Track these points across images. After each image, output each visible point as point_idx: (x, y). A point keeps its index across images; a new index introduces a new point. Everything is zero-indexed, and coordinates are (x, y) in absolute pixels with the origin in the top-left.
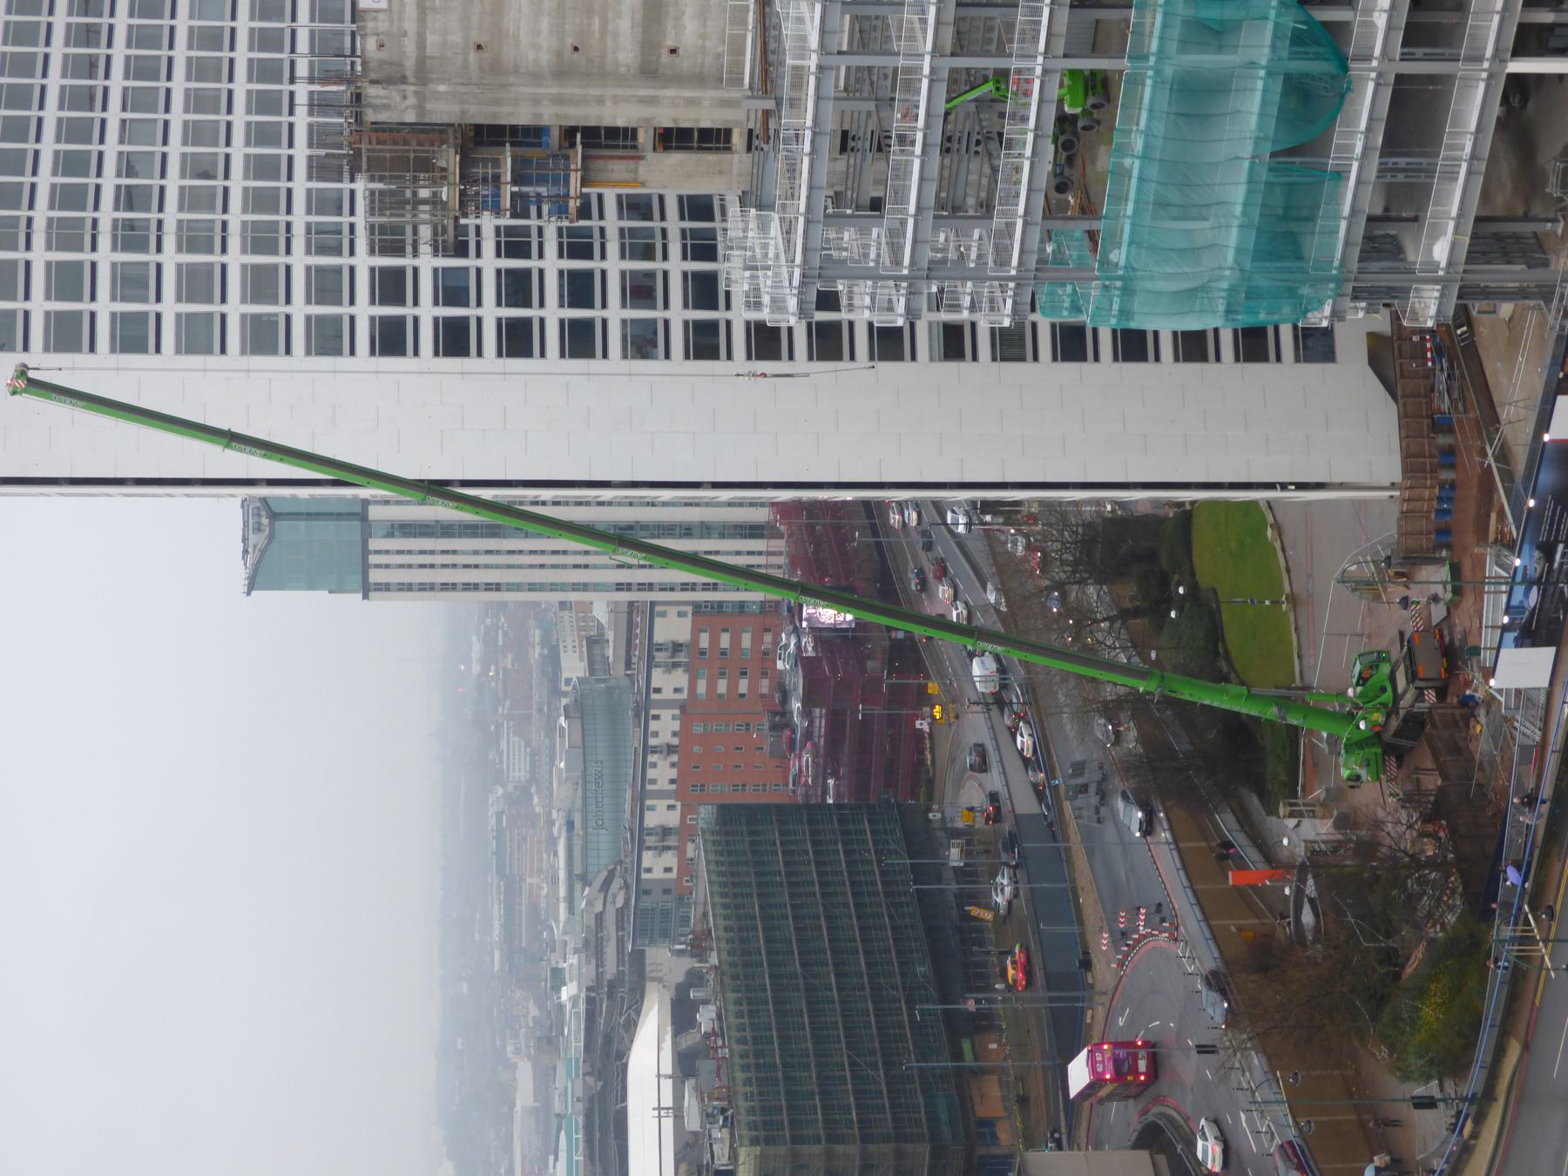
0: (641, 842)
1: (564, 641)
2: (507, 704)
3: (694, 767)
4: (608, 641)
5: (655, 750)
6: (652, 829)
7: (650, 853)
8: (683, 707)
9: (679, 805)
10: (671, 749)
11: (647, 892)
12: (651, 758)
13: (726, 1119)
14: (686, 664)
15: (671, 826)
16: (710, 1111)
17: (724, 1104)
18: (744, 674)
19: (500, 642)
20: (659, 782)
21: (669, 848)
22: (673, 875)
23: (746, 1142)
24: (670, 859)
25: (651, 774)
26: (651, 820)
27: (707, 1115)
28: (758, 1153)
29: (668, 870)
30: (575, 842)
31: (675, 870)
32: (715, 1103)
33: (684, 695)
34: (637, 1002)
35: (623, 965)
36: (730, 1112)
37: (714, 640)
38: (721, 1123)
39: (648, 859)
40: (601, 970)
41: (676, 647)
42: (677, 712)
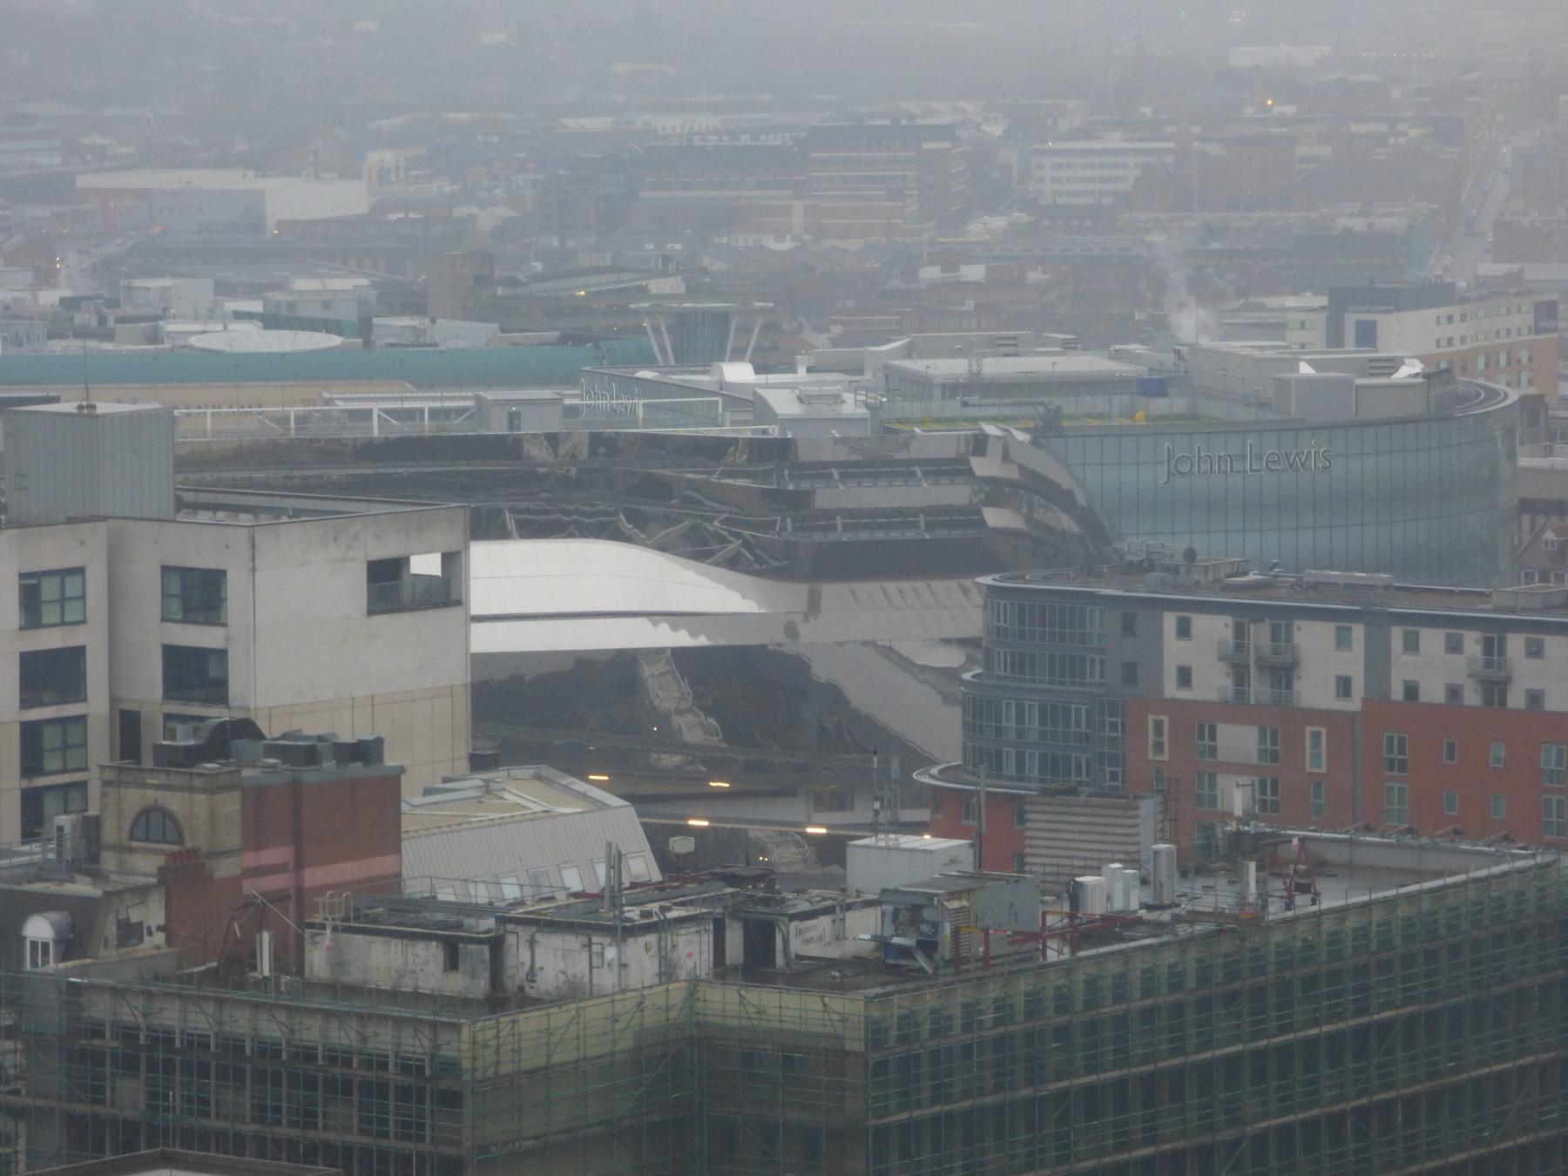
0: (1259, 613)
1: (1463, 318)
2: (1215, 149)
3: (1451, 746)
4: (1549, 452)
5: (1494, 649)
6: (1289, 639)
7: (1229, 634)
9: (1354, 704)
10: (1495, 689)
11: (1129, 628)
12: (1472, 642)
13: (905, 952)
15: (1297, 686)
16: (928, 914)
17: (945, 950)
20: (1409, 658)
21: (1240, 677)
22: (1171, 690)
23: (876, 1013)
24: (1212, 683)
25: (1433, 640)
26: (1313, 639)
27: (916, 909)
28: (849, 1046)
29: (1185, 677)
30: (1116, 399)
31: (1184, 694)
32: (948, 929)
34: (759, 560)
35: (846, 528)
36: (922, 962)
38: (896, 940)
39: (1213, 629)
40: (835, 473)
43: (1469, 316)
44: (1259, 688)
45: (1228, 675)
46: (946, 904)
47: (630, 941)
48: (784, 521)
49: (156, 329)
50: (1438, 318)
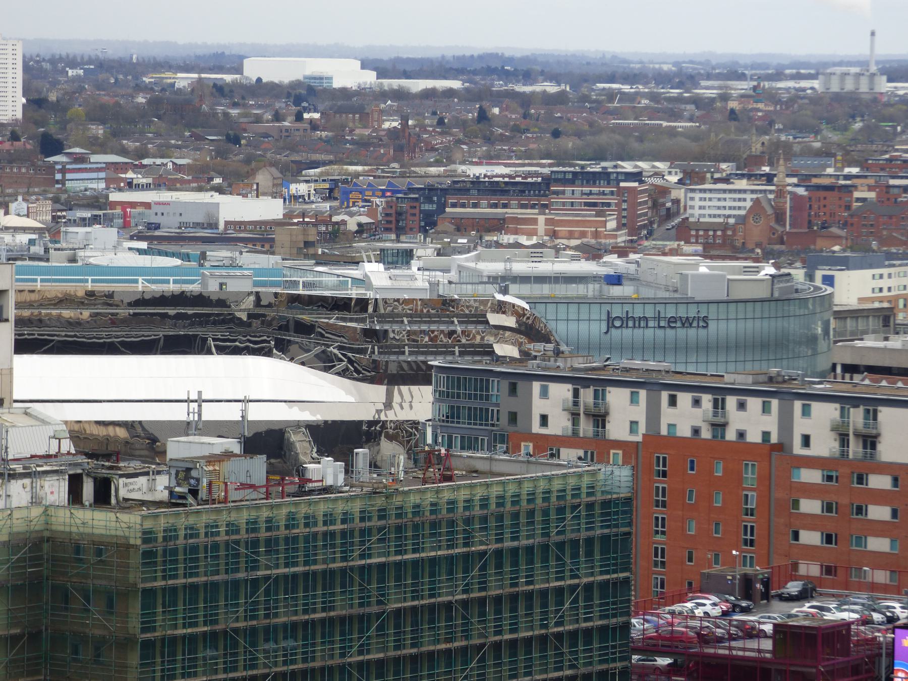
0: (586, 382)
1: (890, 276)
2: (801, 191)
3: (692, 462)
4: (886, 339)
5: (719, 405)
6: (604, 399)
7: (570, 395)
8: (781, 447)
9: (639, 438)
10: (719, 427)
11: (513, 389)
12: (707, 400)
13: (182, 497)
14: (844, 454)
15: (608, 426)
16: (194, 473)
17: (203, 494)
18: (829, 539)
19: (892, 182)
20: (671, 410)
22: (536, 428)
23: (148, 524)
24: (559, 425)
25: (685, 399)
26: (617, 398)
27: (188, 470)
28: (132, 542)
29: (544, 420)
30: (591, 286)
31: (544, 431)
32: (205, 482)
33: (798, 449)
34: (357, 371)
35: (411, 353)
36: (191, 500)
37: (880, 497)
38: (178, 489)
39: (561, 392)
40: (405, 320)
41: (870, 441)
42: (774, 439)
43: (893, 275)
44: (586, 428)
45: (569, 420)
46: (204, 467)
47: (13, 481)
48: (373, 348)
49: (75, 255)
50: (874, 275)
